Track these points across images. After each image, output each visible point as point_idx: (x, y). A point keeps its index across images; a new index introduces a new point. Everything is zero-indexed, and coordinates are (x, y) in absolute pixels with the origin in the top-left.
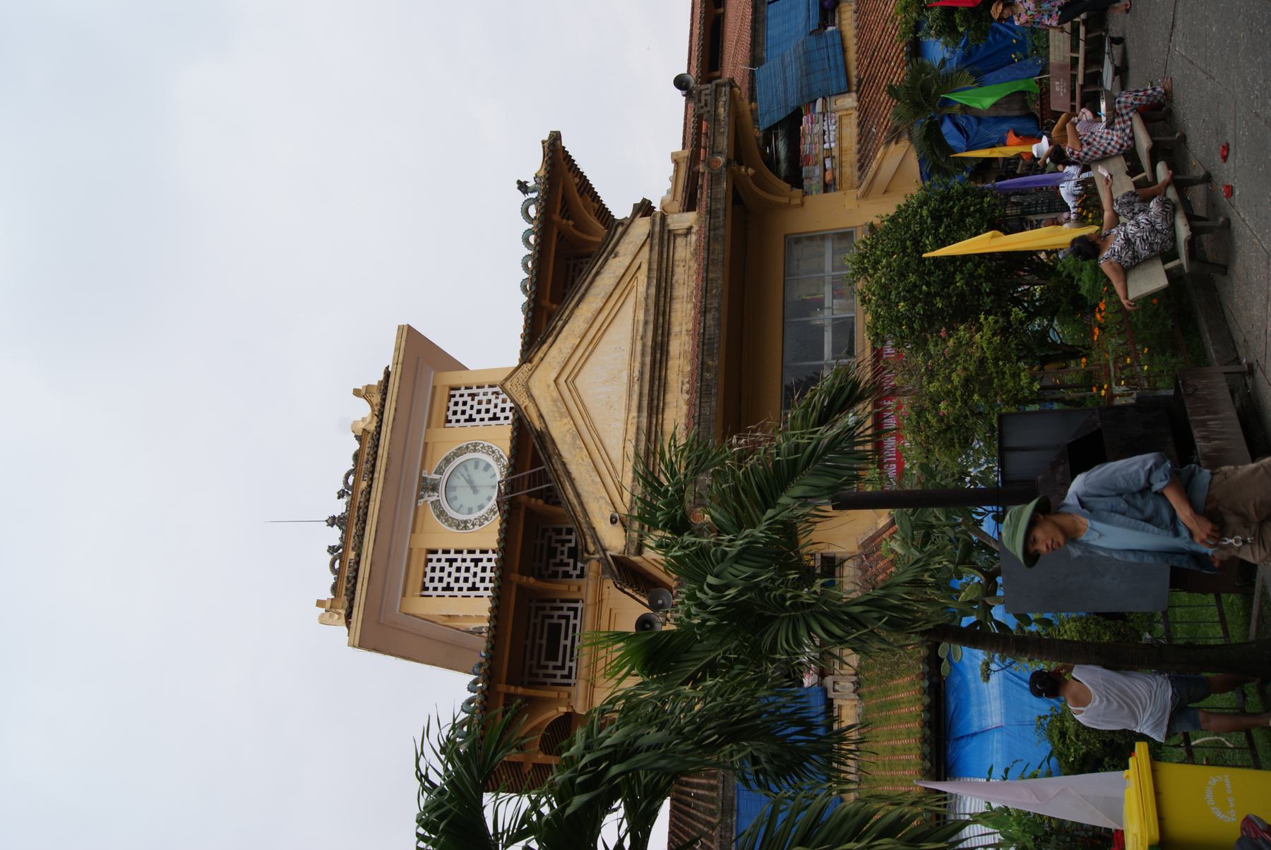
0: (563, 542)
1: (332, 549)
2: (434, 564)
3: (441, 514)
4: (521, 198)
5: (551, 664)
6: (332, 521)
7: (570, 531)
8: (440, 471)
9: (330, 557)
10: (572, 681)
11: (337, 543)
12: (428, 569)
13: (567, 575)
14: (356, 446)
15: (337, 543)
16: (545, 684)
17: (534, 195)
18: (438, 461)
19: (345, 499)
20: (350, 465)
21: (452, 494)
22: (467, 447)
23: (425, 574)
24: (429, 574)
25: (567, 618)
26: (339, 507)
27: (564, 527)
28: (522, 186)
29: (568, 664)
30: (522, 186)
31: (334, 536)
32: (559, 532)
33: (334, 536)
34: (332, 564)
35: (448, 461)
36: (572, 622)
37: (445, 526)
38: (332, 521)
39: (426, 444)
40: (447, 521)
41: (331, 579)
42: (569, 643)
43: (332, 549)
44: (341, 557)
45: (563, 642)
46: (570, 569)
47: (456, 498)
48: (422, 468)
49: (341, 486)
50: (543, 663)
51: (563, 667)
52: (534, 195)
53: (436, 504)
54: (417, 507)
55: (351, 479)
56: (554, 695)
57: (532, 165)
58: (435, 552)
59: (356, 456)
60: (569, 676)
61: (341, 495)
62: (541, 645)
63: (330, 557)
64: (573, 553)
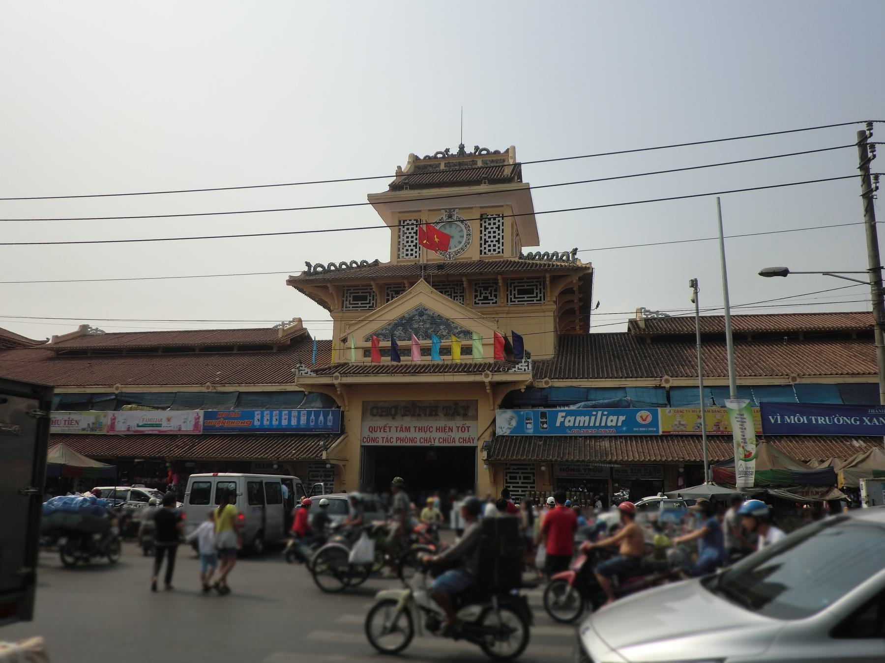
1: (447, 150)
4: (570, 250)
6: (462, 147)
11: (450, 153)
14: (502, 151)
15: (450, 153)
20: (492, 150)
28: (575, 251)
30: (575, 251)
31: (454, 151)
38: (462, 147)
39: (472, 208)
41: (432, 154)
43: (447, 150)
44: (444, 157)
48: (460, 209)
54: (440, 210)
55: (484, 152)
57: (583, 259)
59: (497, 152)
61: (477, 148)
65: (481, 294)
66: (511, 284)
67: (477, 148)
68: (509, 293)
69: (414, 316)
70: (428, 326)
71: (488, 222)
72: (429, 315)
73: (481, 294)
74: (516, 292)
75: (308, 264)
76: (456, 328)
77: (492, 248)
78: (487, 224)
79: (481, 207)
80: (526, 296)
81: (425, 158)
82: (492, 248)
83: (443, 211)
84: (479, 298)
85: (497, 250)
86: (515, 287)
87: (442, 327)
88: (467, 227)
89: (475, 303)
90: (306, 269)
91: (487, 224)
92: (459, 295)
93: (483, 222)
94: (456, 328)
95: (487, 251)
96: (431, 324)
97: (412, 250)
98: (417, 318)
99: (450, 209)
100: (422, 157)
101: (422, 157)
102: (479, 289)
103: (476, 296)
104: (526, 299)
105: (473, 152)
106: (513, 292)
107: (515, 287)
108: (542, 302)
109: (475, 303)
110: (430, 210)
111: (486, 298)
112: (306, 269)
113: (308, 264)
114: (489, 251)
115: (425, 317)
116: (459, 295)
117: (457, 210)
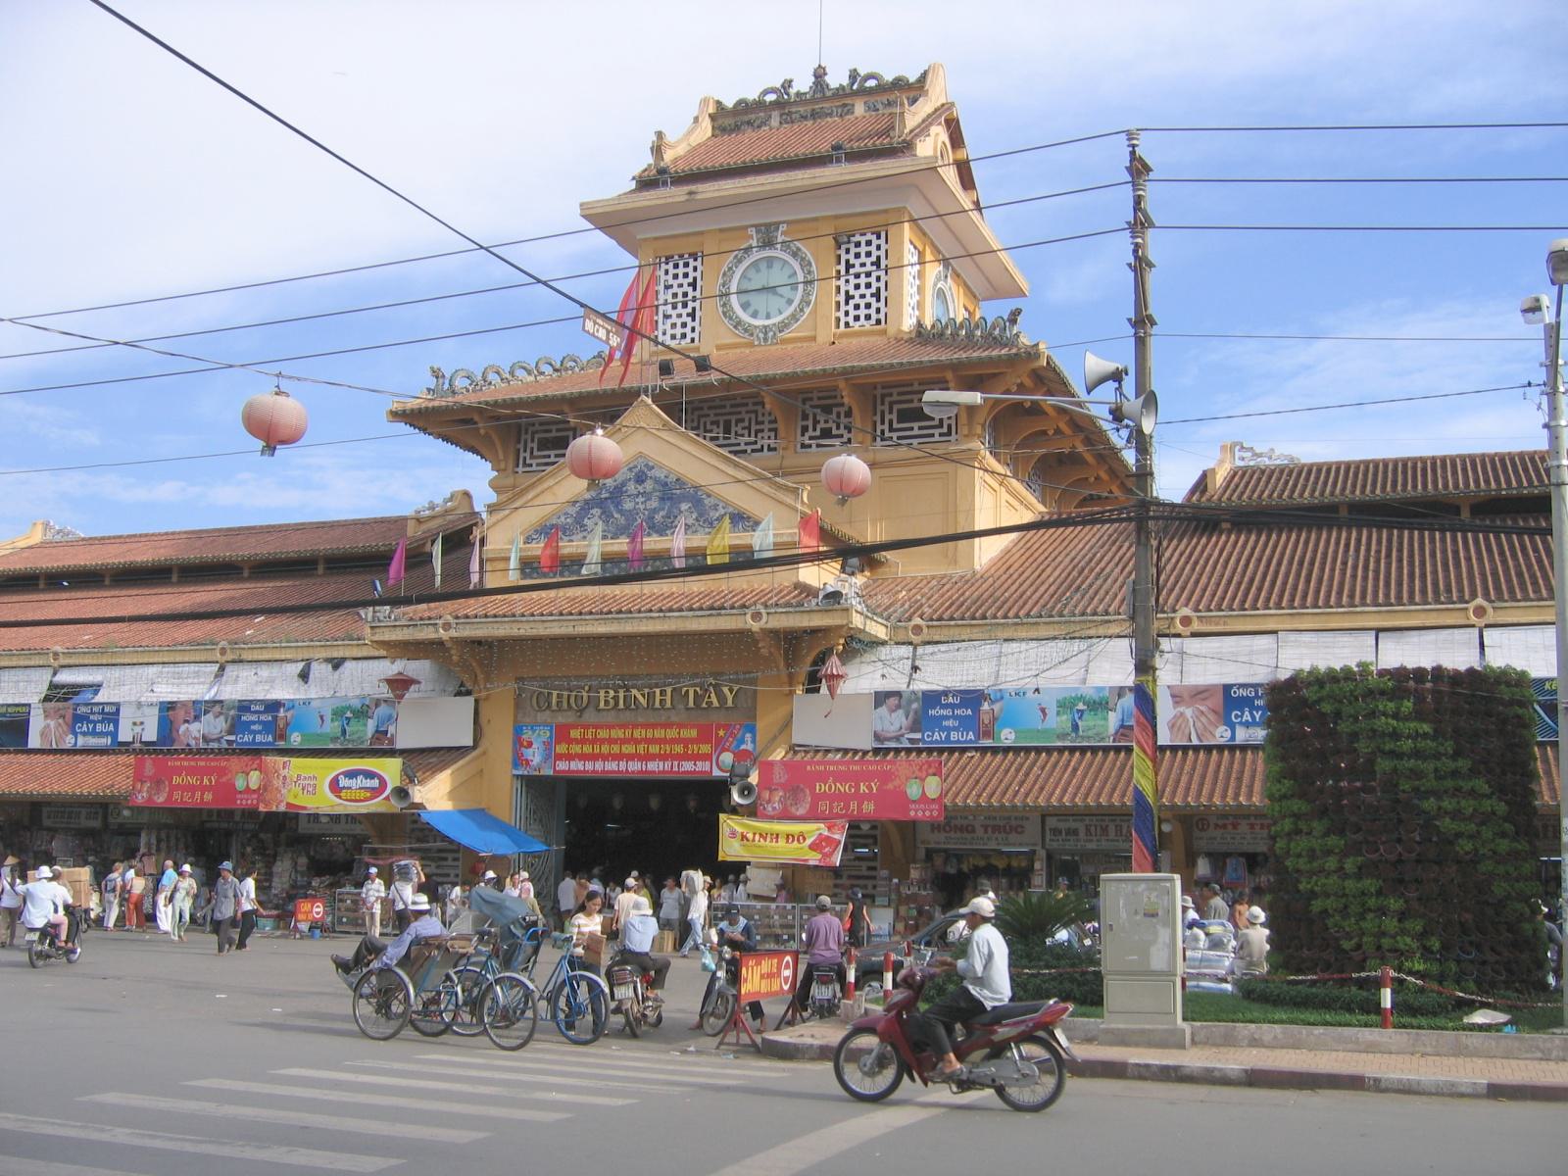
1: (788, 84)
6: (820, 74)
9: (778, 86)
10: (521, 469)
15: (792, 91)
16: (519, 442)
19: (845, 82)
20: (889, 77)
21: (763, 266)
22: (809, 272)
23: (681, 256)
26: (836, 79)
31: (803, 84)
34: (772, 90)
38: (820, 74)
40: (730, 269)
41: (752, 95)
43: (788, 84)
47: (758, 271)
48: (788, 223)
49: (862, 72)
50: (537, 436)
51: (532, 456)
54: (746, 228)
55: (872, 83)
56: (501, 457)
60: (525, 464)
62: (550, 431)
63: (778, 86)
65: (816, 422)
66: (883, 396)
67: (854, 75)
68: (878, 418)
69: (623, 484)
70: (654, 504)
71: (853, 250)
72: (656, 480)
73: (816, 422)
74: (894, 417)
75: (437, 374)
76: (715, 507)
77: (862, 312)
78: (851, 257)
79: (836, 217)
80: (916, 425)
81: (739, 102)
82: (862, 312)
83: (752, 231)
84: (811, 433)
85: (874, 317)
86: (891, 405)
87: (684, 506)
88: (805, 264)
89: (803, 446)
90: (432, 383)
91: (851, 257)
92: (766, 426)
93: (842, 252)
94: (715, 507)
95: (850, 319)
96: (662, 499)
97: (684, 325)
98: (631, 487)
99: (768, 226)
100: (729, 103)
101: (729, 103)
102: (810, 412)
103: (805, 429)
104: (916, 432)
105: (845, 82)
106: (887, 417)
107: (891, 405)
108: (953, 437)
109: (803, 446)
110: (722, 230)
111: (826, 434)
112: (432, 383)
113: (437, 374)
114: (857, 318)
115: (649, 485)
116: (766, 426)
117: (783, 228)
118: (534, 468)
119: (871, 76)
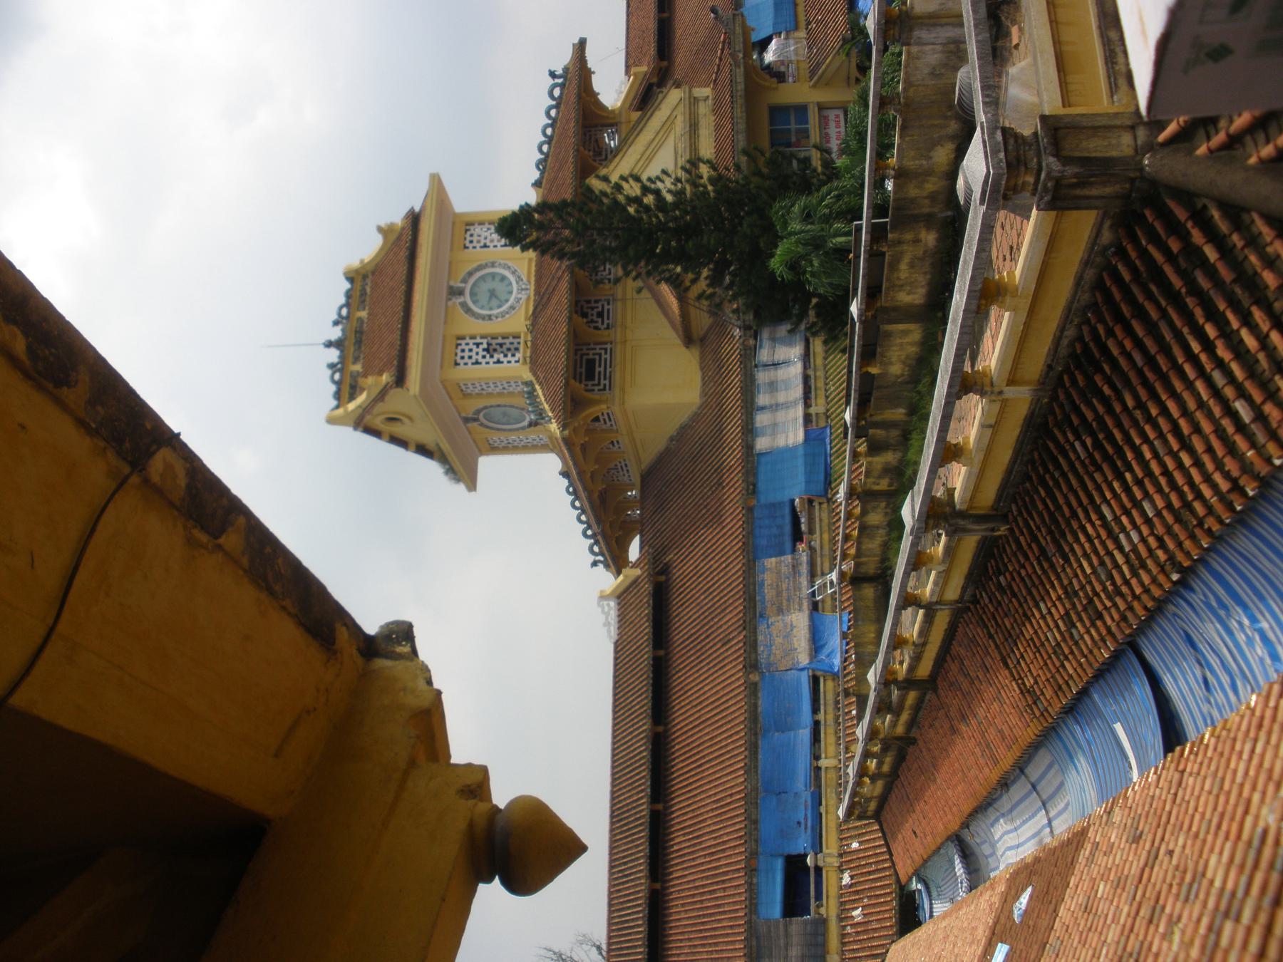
0: (592, 308)
2: (463, 346)
3: (468, 310)
4: (551, 81)
5: (590, 383)
6: (329, 344)
7: (596, 302)
8: (464, 281)
9: (329, 372)
12: (459, 351)
13: (597, 328)
14: (347, 285)
17: (560, 81)
18: (462, 274)
19: (339, 328)
20: (343, 300)
24: (460, 354)
25: (600, 355)
26: (336, 333)
27: (593, 299)
28: (553, 75)
29: (602, 382)
30: (553, 75)
31: (333, 355)
32: (589, 302)
33: (333, 355)
35: (470, 274)
36: (603, 356)
37: (473, 319)
38: (329, 344)
39: (450, 263)
41: (333, 388)
42: (602, 369)
43: (331, 366)
44: (341, 371)
45: (597, 369)
46: (599, 325)
49: (335, 317)
52: (560, 81)
53: (464, 305)
57: (562, 58)
58: (463, 338)
59: (349, 295)
61: (336, 323)
64: (600, 315)
67: (336, 323)
83: (450, 303)
105: (339, 328)
117: (452, 283)
118: (607, 382)
119: (341, 308)
